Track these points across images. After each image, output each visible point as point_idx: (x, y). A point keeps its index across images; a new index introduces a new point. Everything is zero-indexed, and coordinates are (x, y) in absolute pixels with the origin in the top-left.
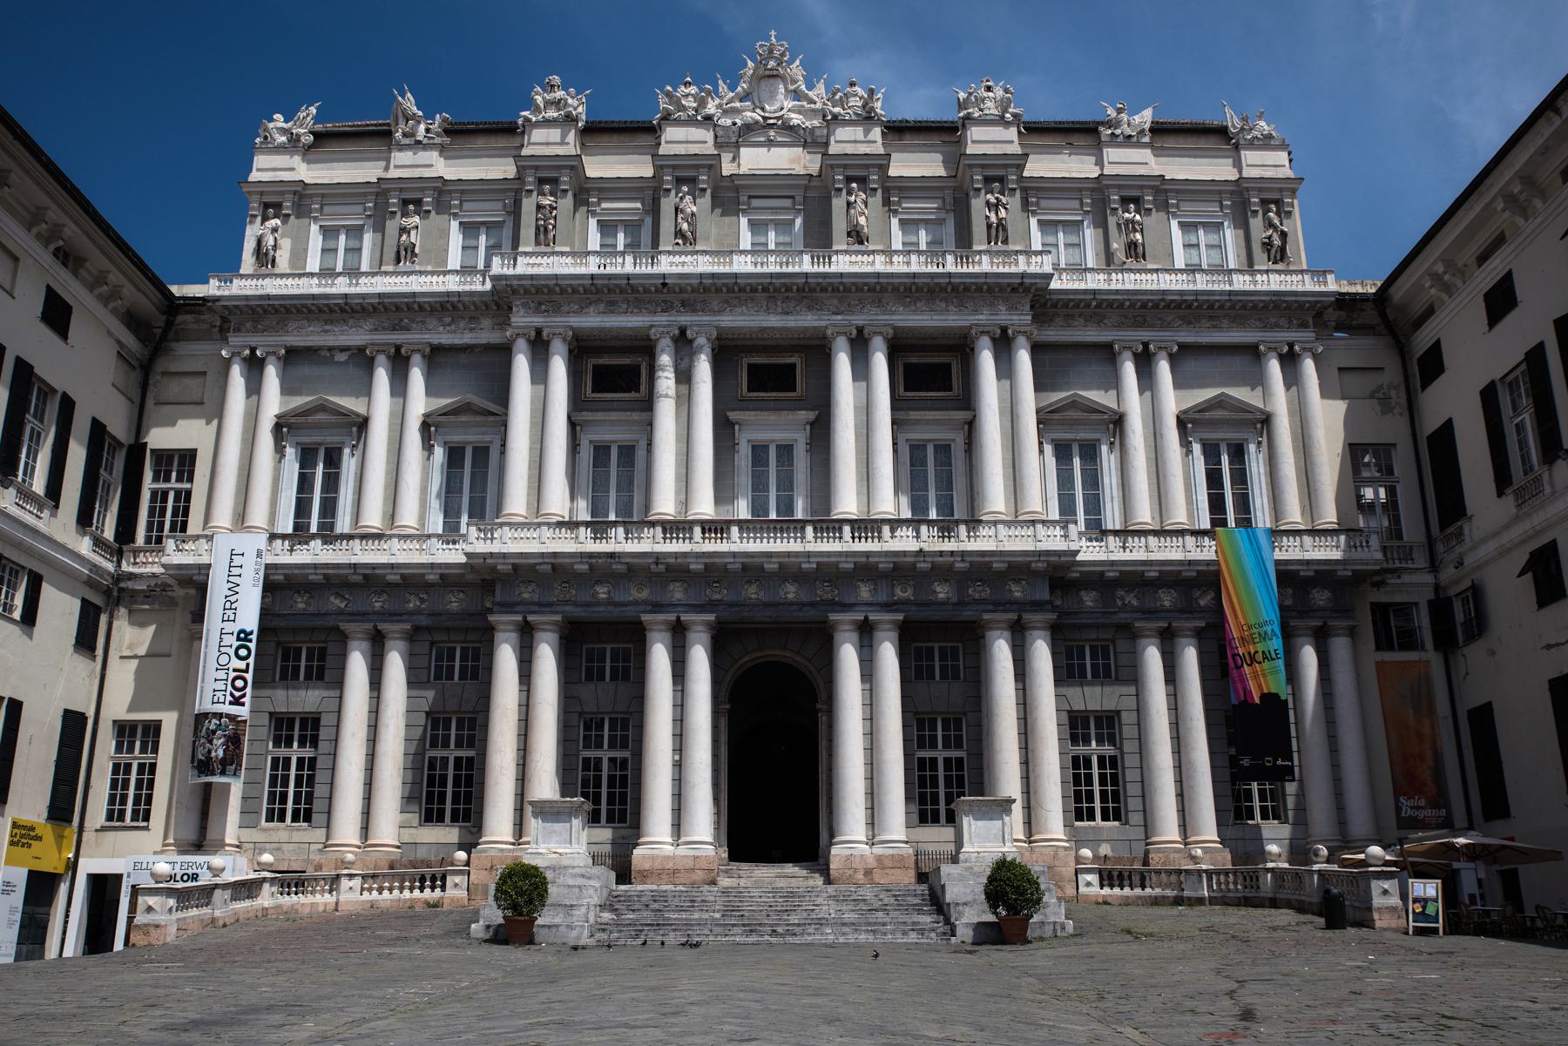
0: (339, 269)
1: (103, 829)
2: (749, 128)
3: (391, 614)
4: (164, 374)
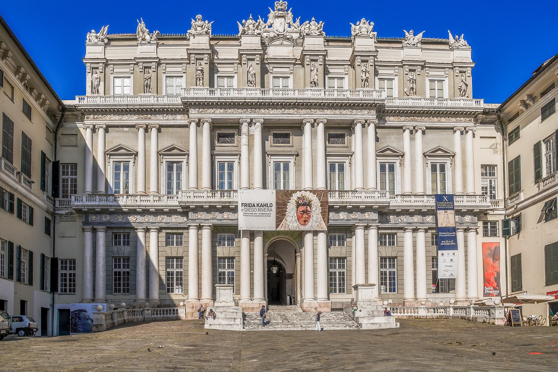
1: (60, 294)
2: (272, 39)
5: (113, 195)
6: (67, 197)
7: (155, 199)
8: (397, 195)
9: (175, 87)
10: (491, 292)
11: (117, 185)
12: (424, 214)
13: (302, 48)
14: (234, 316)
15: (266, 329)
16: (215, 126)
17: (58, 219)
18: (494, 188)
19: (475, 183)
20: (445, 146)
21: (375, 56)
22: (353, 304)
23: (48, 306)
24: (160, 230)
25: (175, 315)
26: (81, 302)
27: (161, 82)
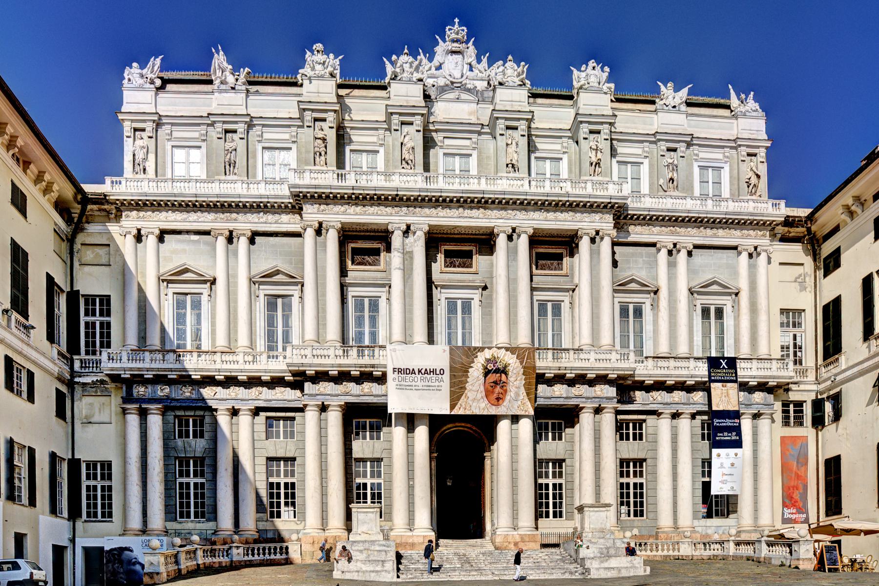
1: (85, 521)
5: (174, 351)
6: (94, 353)
7: (246, 359)
8: (646, 358)
10: (793, 517)
11: (181, 334)
12: (690, 389)
13: (492, 107)
14: (383, 557)
15: (435, 577)
16: (347, 235)
17: (78, 390)
18: (800, 348)
19: (772, 339)
21: (611, 124)
22: (577, 536)
23: (64, 542)
25: (284, 556)
26: (123, 535)
27: (255, 157)
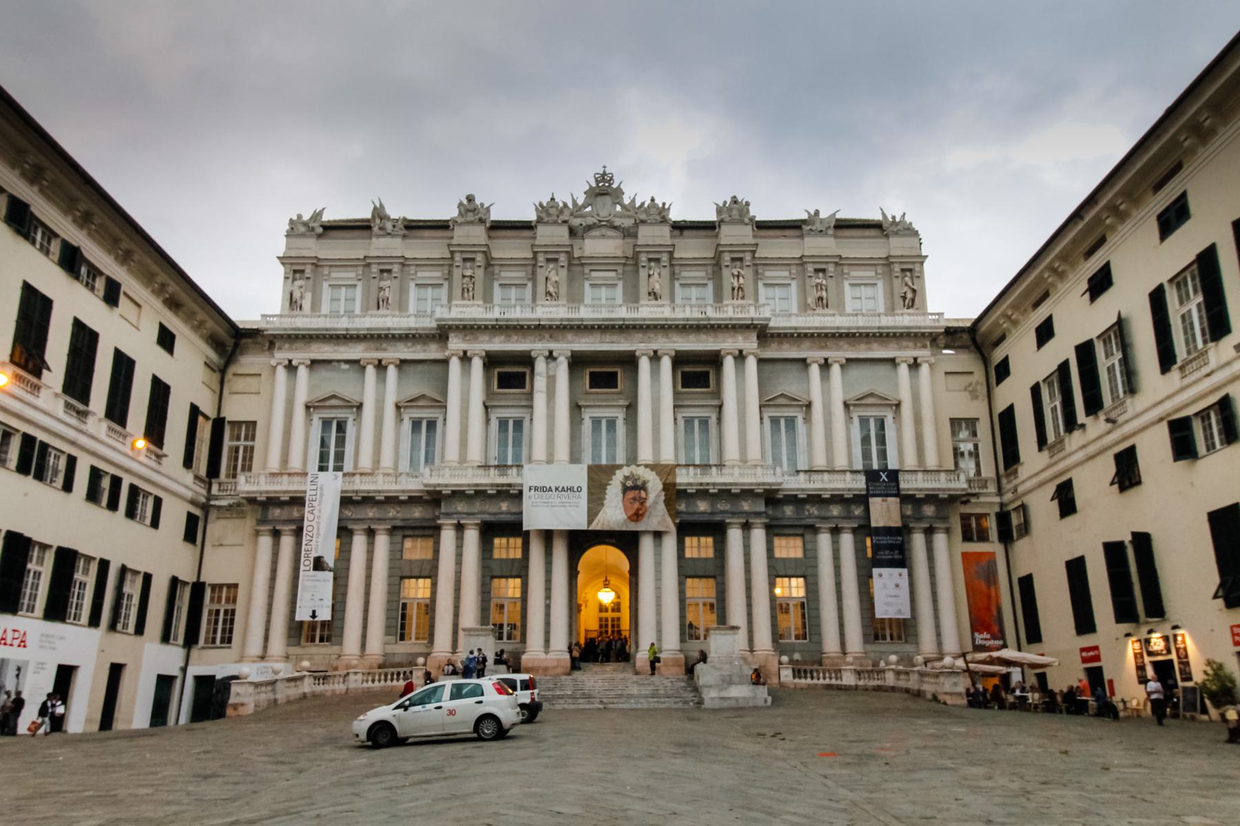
0: (342, 312)
1: (203, 648)
2: (590, 228)
3: (379, 519)
4: (235, 375)
9: (429, 301)
16: (491, 361)
17: (213, 515)
20: (881, 390)
24: (393, 531)
27: (407, 292)
